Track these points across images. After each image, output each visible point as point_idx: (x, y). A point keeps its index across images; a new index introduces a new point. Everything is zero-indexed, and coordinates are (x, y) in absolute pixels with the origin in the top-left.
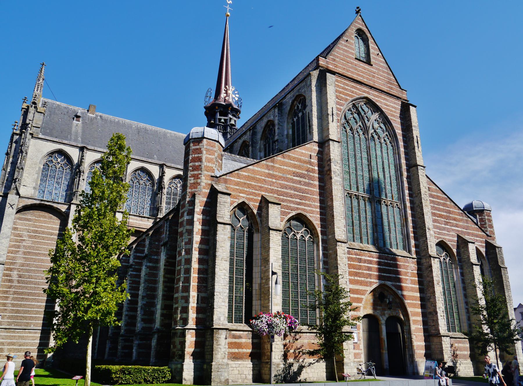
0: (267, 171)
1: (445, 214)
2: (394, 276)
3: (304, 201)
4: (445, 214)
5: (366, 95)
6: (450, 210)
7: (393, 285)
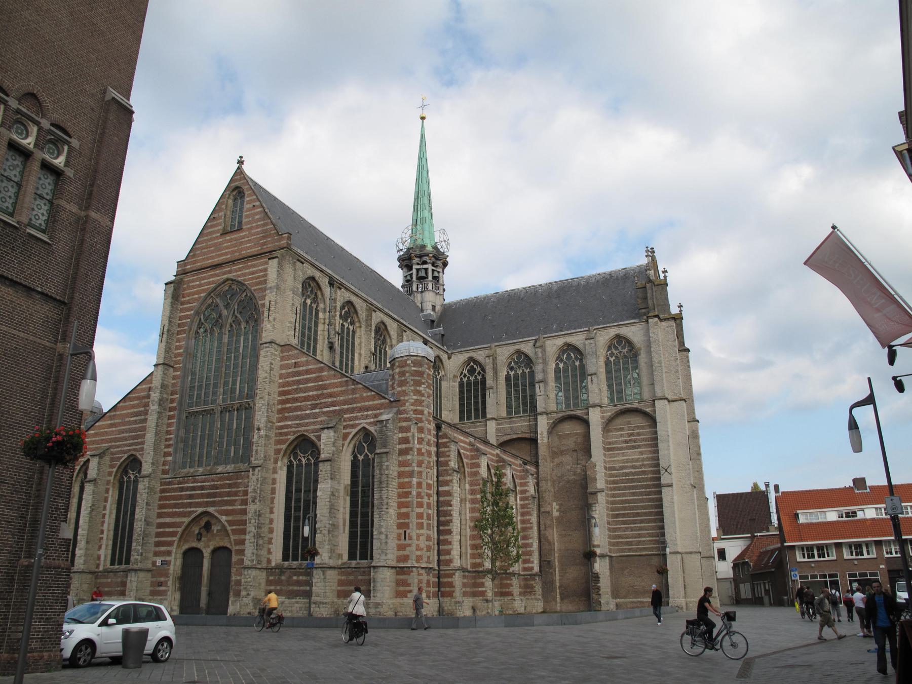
0: (109, 422)
1: (315, 393)
2: (220, 499)
3: (136, 441)
4: (315, 393)
5: (225, 277)
6: (325, 385)
7: (215, 511)
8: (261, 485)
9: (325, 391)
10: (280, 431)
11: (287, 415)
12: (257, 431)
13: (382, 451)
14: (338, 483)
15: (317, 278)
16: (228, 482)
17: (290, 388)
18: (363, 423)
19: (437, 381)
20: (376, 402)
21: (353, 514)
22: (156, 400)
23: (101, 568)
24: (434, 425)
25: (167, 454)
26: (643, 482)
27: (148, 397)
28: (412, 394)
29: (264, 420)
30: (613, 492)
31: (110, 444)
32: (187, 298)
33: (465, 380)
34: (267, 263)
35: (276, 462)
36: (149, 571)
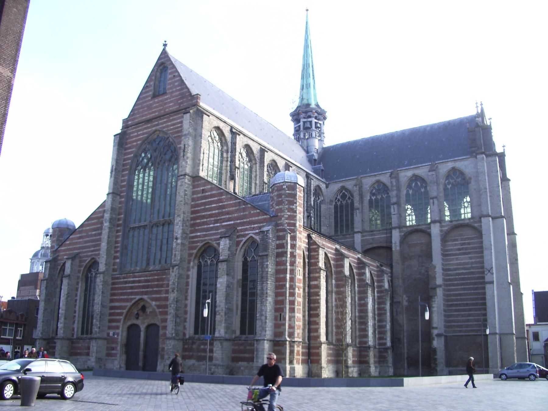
0: (78, 235)
1: (217, 211)
2: (151, 289)
3: (96, 248)
4: (217, 211)
5: (154, 128)
6: (224, 205)
8: (178, 279)
9: (224, 210)
10: (192, 240)
11: (197, 228)
12: (175, 240)
13: (263, 254)
14: (233, 278)
15: (221, 128)
16: (156, 277)
17: (199, 208)
18: (251, 233)
19: (317, 204)
20: (260, 218)
21: (244, 301)
22: (108, 219)
23: (75, 337)
24: (306, 235)
25: (116, 258)
26: (472, 280)
27: (103, 217)
28: (286, 211)
29: (180, 232)
30: (448, 288)
31: (79, 251)
32: (129, 145)
33: (339, 203)
34: (182, 117)
35: (189, 263)
36: (105, 339)
